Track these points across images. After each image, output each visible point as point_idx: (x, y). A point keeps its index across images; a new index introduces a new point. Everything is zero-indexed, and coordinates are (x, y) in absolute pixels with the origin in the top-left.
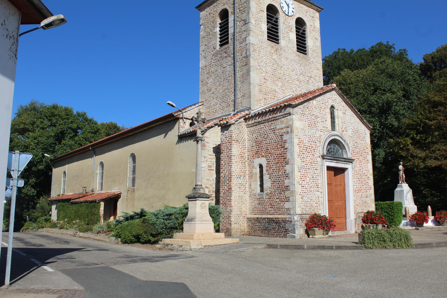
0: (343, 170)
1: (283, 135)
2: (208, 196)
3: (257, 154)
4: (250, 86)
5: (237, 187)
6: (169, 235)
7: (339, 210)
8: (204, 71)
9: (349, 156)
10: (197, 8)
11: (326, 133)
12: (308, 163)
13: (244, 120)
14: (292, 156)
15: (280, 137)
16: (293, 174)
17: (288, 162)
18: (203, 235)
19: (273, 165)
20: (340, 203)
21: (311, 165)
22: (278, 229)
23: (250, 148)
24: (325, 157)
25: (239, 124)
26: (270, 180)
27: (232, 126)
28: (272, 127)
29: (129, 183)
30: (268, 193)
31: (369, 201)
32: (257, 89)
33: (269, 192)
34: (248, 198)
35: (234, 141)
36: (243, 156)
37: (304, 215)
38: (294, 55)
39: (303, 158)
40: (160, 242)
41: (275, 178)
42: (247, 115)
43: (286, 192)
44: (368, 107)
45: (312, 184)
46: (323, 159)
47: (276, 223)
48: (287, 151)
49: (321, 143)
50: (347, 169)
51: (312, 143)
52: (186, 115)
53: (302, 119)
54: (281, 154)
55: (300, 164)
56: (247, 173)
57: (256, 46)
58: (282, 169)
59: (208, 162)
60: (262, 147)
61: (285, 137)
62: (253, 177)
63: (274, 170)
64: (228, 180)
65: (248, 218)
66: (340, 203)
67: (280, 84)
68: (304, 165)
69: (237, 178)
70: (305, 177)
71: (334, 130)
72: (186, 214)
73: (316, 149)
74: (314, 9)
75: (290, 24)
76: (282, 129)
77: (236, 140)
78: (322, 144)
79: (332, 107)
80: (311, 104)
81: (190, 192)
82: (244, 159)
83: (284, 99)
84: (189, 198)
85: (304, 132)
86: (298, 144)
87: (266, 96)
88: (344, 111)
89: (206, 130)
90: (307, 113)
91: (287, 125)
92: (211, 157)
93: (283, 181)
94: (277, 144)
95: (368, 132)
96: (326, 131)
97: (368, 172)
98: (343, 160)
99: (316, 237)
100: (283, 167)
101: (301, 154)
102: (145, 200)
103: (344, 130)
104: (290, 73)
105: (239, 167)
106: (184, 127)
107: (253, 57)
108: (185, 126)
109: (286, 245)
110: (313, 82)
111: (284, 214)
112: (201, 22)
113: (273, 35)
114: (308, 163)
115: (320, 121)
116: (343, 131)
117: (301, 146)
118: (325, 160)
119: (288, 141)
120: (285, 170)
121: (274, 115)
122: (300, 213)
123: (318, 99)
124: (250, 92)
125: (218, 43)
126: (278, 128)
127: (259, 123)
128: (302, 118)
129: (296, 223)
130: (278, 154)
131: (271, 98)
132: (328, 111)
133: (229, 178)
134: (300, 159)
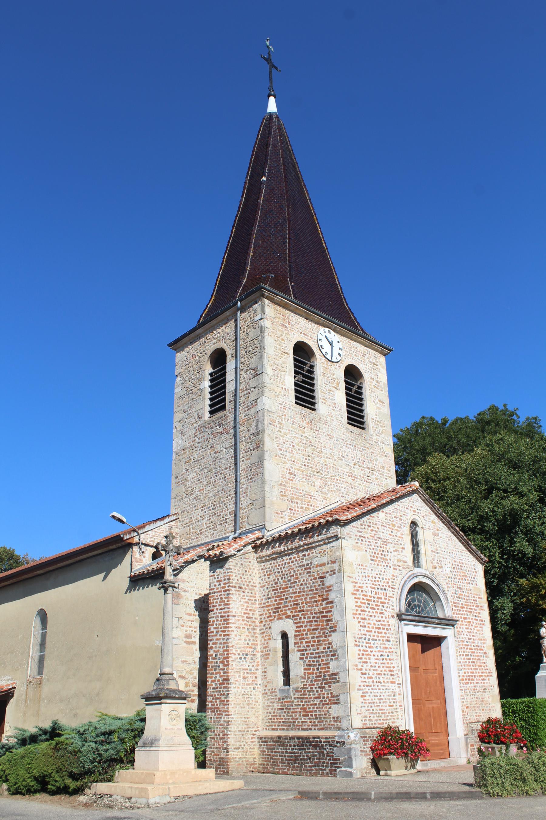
0: (437, 641)
1: (324, 577)
2: (183, 695)
3: (278, 612)
4: (264, 487)
5: (240, 676)
6: (107, 776)
7: (434, 718)
8: (180, 457)
9: (448, 613)
10: (170, 345)
11: (404, 571)
12: (373, 628)
13: (253, 548)
14: (342, 617)
15: (319, 580)
16: (344, 650)
17: (336, 627)
18: (173, 773)
19: (307, 634)
20: (435, 705)
21: (378, 632)
22: (319, 759)
23: (265, 601)
24: (404, 617)
25: (244, 556)
26: (302, 662)
27: (231, 560)
28: (305, 562)
29: (31, 668)
30: (298, 688)
31: (490, 700)
32: (276, 491)
33: (300, 685)
34: (261, 697)
35: (233, 589)
36: (251, 616)
37: (367, 731)
38: (343, 430)
39: (362, 619)
40: (86, 791)
41: (311, 658)
42: (258, 539)
43: (333, 685)
44: (478, 521)
45: (381, 669)
46: (401, 620)
47: (316, 746)
48: (332, 607)
49: (396, 591)
50: (445, 638)
51: (380, 591)
52: (145, 538)
53: (359, 547)
54: (323, 612)
55: (357, 632)
56: (259, 648)
57: (275, 415)
58: (324, 641)
59: (185, 628)
60: (287, 598)
61: (329, 581)
62: (270, 656)
63: (310, 642)
64: (222, 662)
65: (261, 738)
66: (435, 705)
67: (318, 483)
68: (365, 632)
69: (241, 658)
70: (368, 655)
71: (418, 567)
72: (142, 731)
73: (387, 601)
74: (377, 351)
75: (335, 376)
76: (323, 565)
77: (237, 585)
78: (397, 592)
79: (414, 524)
80: (376, 518)
81: (149, 687)
82: (253, 622)
83: (326, 509)
84: (147, 699)
85: (363, 571)
86: (353, 594)
87: (293, 505)
88: (435, 531)
89: (182, 567)
90: (368, 535)
91: (333, 558)
92: (191, 618)
93: (327, 664)
94: (314, 594)
95: (480, 569)
96: (404, 568)
97: (484, 643)
98: (437, 621)
99: (393, 773)
100: (326, 637)
101: (359, 612)
102: (61, 701)
103: (437, 565)
104: (336, 463)
105: (243, 637)
106: (140, 561)
107: (269, 435)
108: (144, 559)
109: (336, 793)
110: (377, 479)
111: (330, 729)
112: (178, 370)
113: (305, 395)
114: (373, 628)
115: (392, 550)
116: (435, 568)
117: (358, 596)
118: (403, 622)
119: (334, 588)
120: (330, 643)
121: (309, 540)
122: (361, 726)
123: (386, 509)
124: (263, 497)
125: (208, 409)
126: (315, 563)
127: (281, 554)
128: (359, 544)
129: (353, 746)
130: (316, 613)
131: (302, 508)
132: (406, 531)
133: (224, 658)
134: (357, 621)
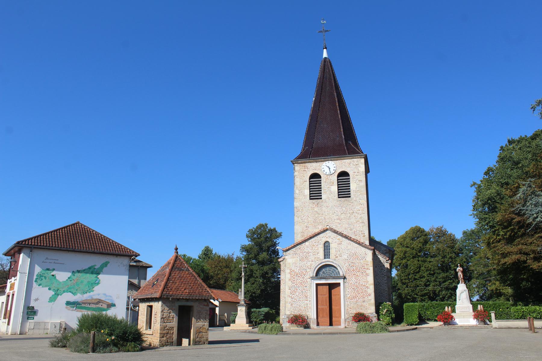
71: (329, 258)
113: (315, 193)
123: (310, 241)
